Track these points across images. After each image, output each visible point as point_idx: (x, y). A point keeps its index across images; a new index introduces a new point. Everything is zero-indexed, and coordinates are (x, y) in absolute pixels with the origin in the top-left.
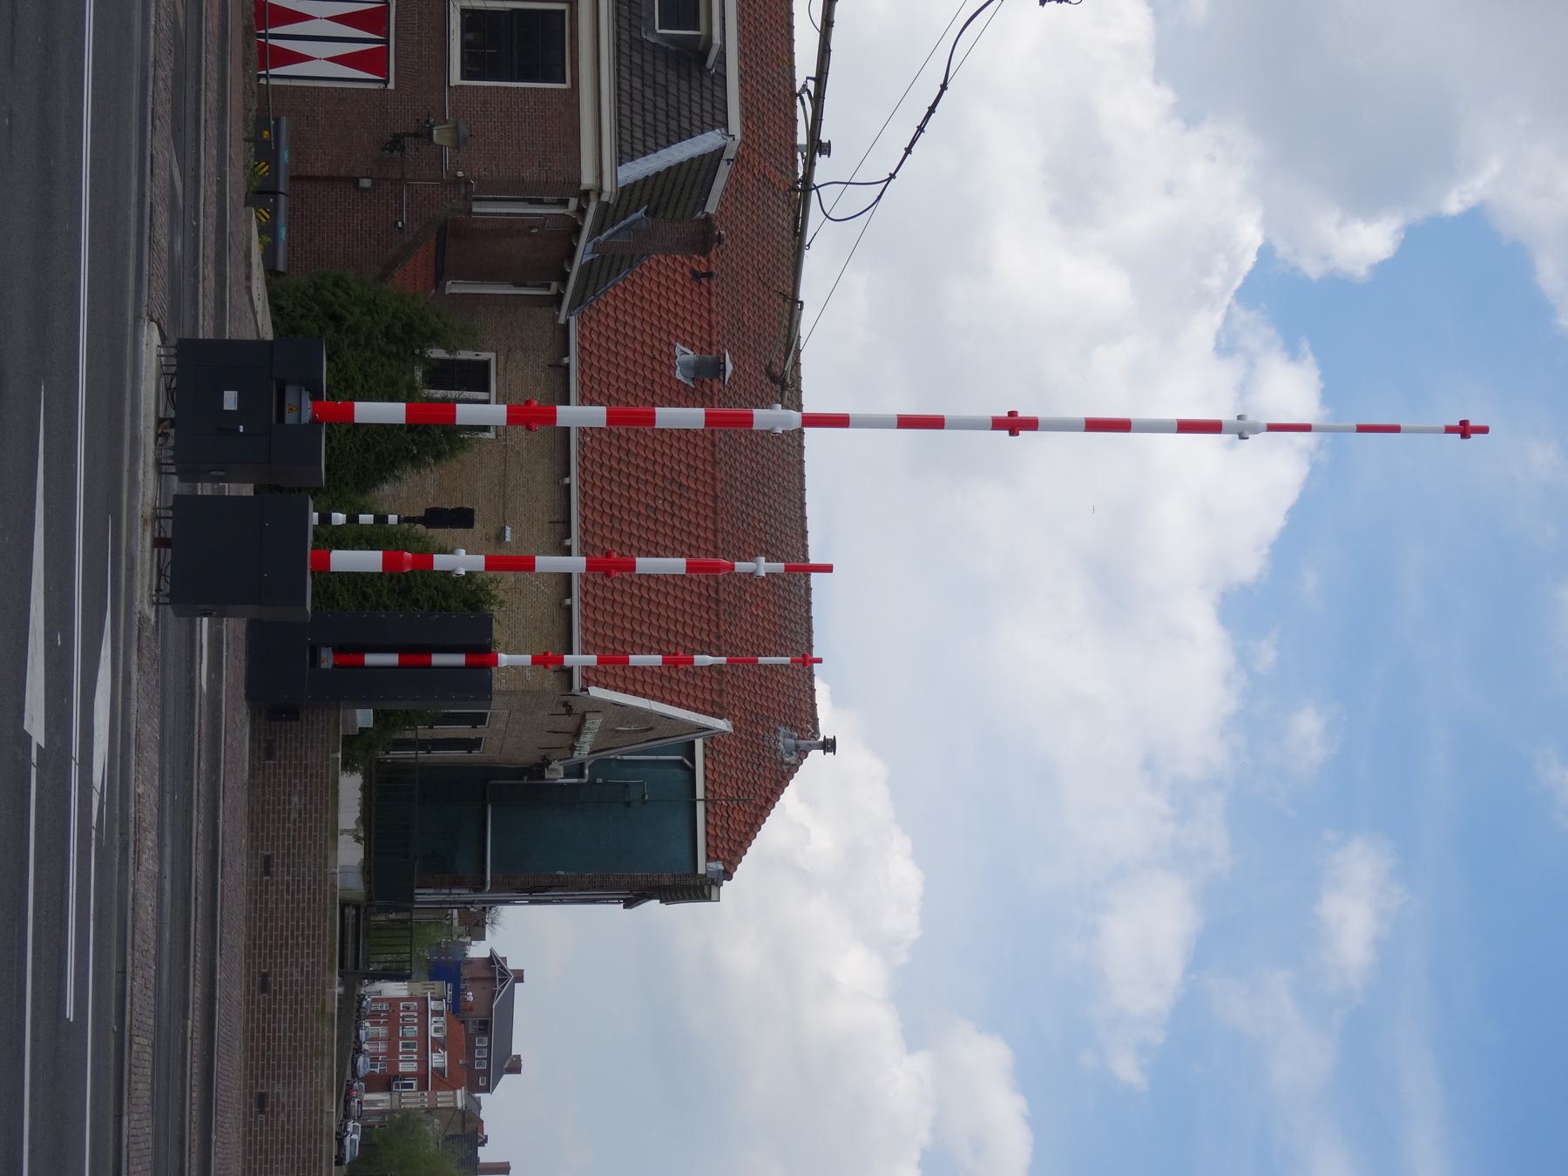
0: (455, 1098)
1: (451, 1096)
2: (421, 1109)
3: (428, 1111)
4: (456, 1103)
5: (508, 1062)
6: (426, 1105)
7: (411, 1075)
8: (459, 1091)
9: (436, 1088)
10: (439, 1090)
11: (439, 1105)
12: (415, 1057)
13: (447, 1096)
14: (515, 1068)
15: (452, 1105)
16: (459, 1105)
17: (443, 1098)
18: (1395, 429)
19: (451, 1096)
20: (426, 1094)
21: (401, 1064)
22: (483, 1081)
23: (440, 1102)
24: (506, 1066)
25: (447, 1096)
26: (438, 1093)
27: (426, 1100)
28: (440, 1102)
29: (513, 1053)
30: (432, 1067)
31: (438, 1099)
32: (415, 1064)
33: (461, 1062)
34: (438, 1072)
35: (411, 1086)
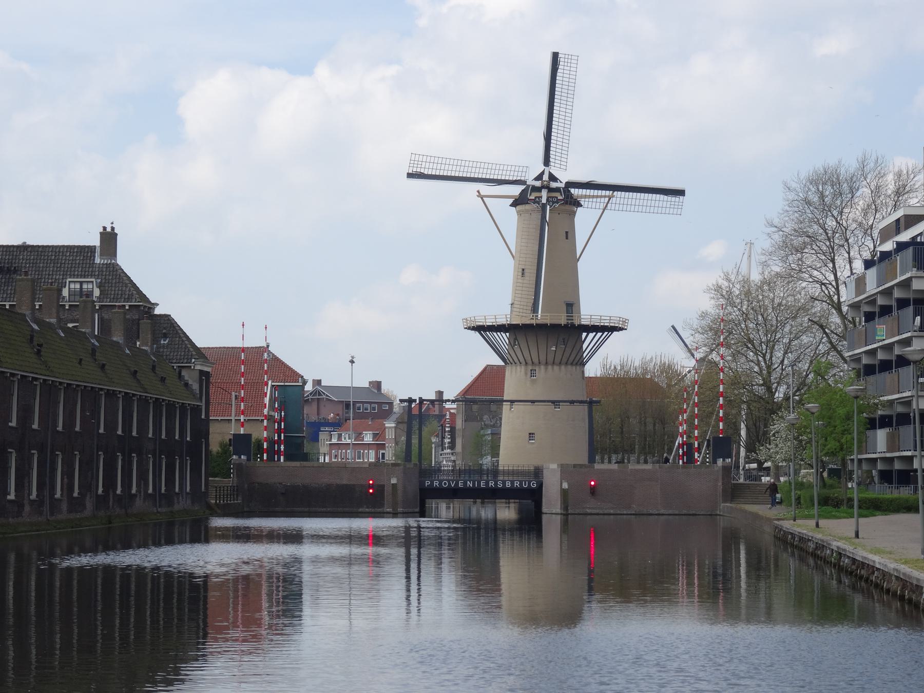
0: (390, 427)
1: (389, 430)
3: (397, 443)
4: (392, 427)
5: (373, 390)
7: (377, 454)
8: (386, 425)
10: (385, 436)
11: (393, 437)
12: (366, 451)
13: (389, 432)
14: (377, 385)
15: (393, 429)
16: (393, 425)
17: (390, 435)
19: (389, 430)
20: (387, 445)
21: (370, 460)
23: (392, 436)
24: (376, 391)
25: (389, 432)
26: (387, 438)
27: (390, 445)
28: (392, 436)
29: (368, 386)
30: (372, 441)
31: (390, 437)
32: (370, 451)
33: (370, 423)
34: (375, 436)
35: (383, 454)
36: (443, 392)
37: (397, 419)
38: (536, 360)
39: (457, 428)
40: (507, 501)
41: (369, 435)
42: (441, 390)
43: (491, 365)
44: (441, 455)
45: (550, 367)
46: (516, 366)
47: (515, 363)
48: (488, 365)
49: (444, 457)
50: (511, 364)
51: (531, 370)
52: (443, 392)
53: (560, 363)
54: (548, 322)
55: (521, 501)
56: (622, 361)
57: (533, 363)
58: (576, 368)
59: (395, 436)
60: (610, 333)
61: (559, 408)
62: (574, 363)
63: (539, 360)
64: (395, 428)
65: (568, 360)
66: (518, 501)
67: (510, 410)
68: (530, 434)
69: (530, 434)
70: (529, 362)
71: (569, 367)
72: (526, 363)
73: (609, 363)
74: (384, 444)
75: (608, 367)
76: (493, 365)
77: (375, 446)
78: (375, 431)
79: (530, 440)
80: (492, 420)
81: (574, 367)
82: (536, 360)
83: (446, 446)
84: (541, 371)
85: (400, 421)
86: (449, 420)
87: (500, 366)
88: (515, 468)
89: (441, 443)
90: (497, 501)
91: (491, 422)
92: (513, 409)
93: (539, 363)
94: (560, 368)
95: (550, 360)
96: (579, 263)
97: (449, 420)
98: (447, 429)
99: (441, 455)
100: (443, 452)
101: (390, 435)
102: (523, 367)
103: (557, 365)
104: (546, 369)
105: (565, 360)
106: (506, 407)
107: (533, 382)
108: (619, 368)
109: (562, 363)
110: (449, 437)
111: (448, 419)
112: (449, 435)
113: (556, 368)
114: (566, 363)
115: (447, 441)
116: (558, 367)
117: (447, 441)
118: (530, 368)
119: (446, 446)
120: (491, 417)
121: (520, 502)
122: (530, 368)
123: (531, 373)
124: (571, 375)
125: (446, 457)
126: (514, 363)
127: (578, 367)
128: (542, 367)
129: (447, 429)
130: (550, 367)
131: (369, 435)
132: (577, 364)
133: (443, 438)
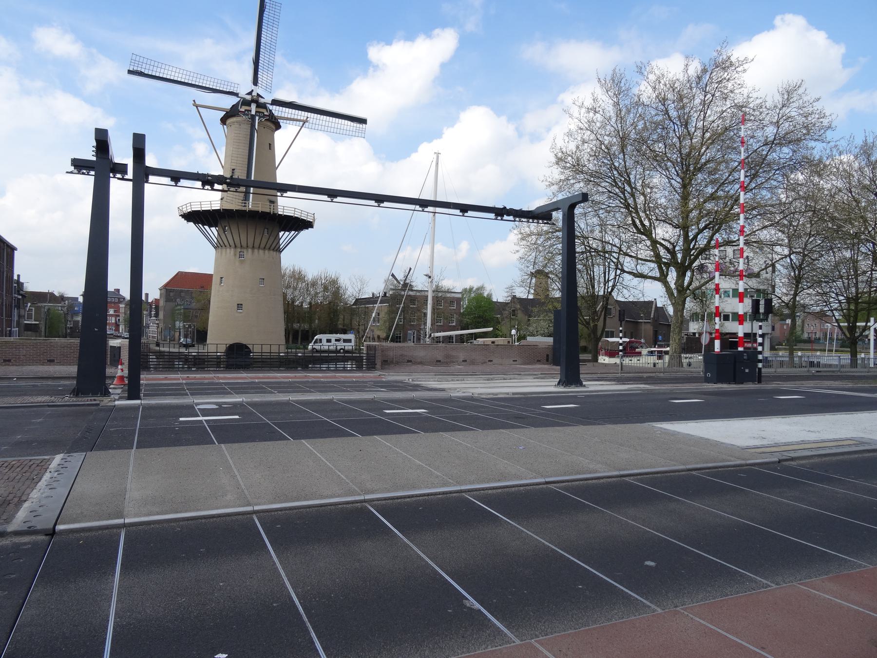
3: (125, 314)
16: (124, 306)
17: (122, 310)
34: (115, 311)
35: (119, 319)
38: (244, 244)
45: (256, 251)
46: (226, 249)
47: (225, 246)
53: (265, 248)
57: (241, 246)
62: (275, 249)
65: (271, 246)
69: (238, 304)
71: (272, 252)
79: (238, 309)
81: (275, 253)
82: (244, 244)
84: (248, 254)
92: (222, 284)
93: (247, 247)
94: (264, 253)
95: (257, 245)
96: (278, 171)
101: (122, 310)
102: (232, 249)
103: (262, 249)
104: (253, 252)
105: (268, 246)
107: (242, 262)
109: (266, 248)
113: (261, 251)
114: (269, 249)
115: (153, 313)
116: (263, 251)
118: (239, 250)
122: (239, 250)
123: (240, 255)
124: (273, 258)
126: (224, 246)
128: (250, 250)
130: (256, 251)
133: (151, 311)
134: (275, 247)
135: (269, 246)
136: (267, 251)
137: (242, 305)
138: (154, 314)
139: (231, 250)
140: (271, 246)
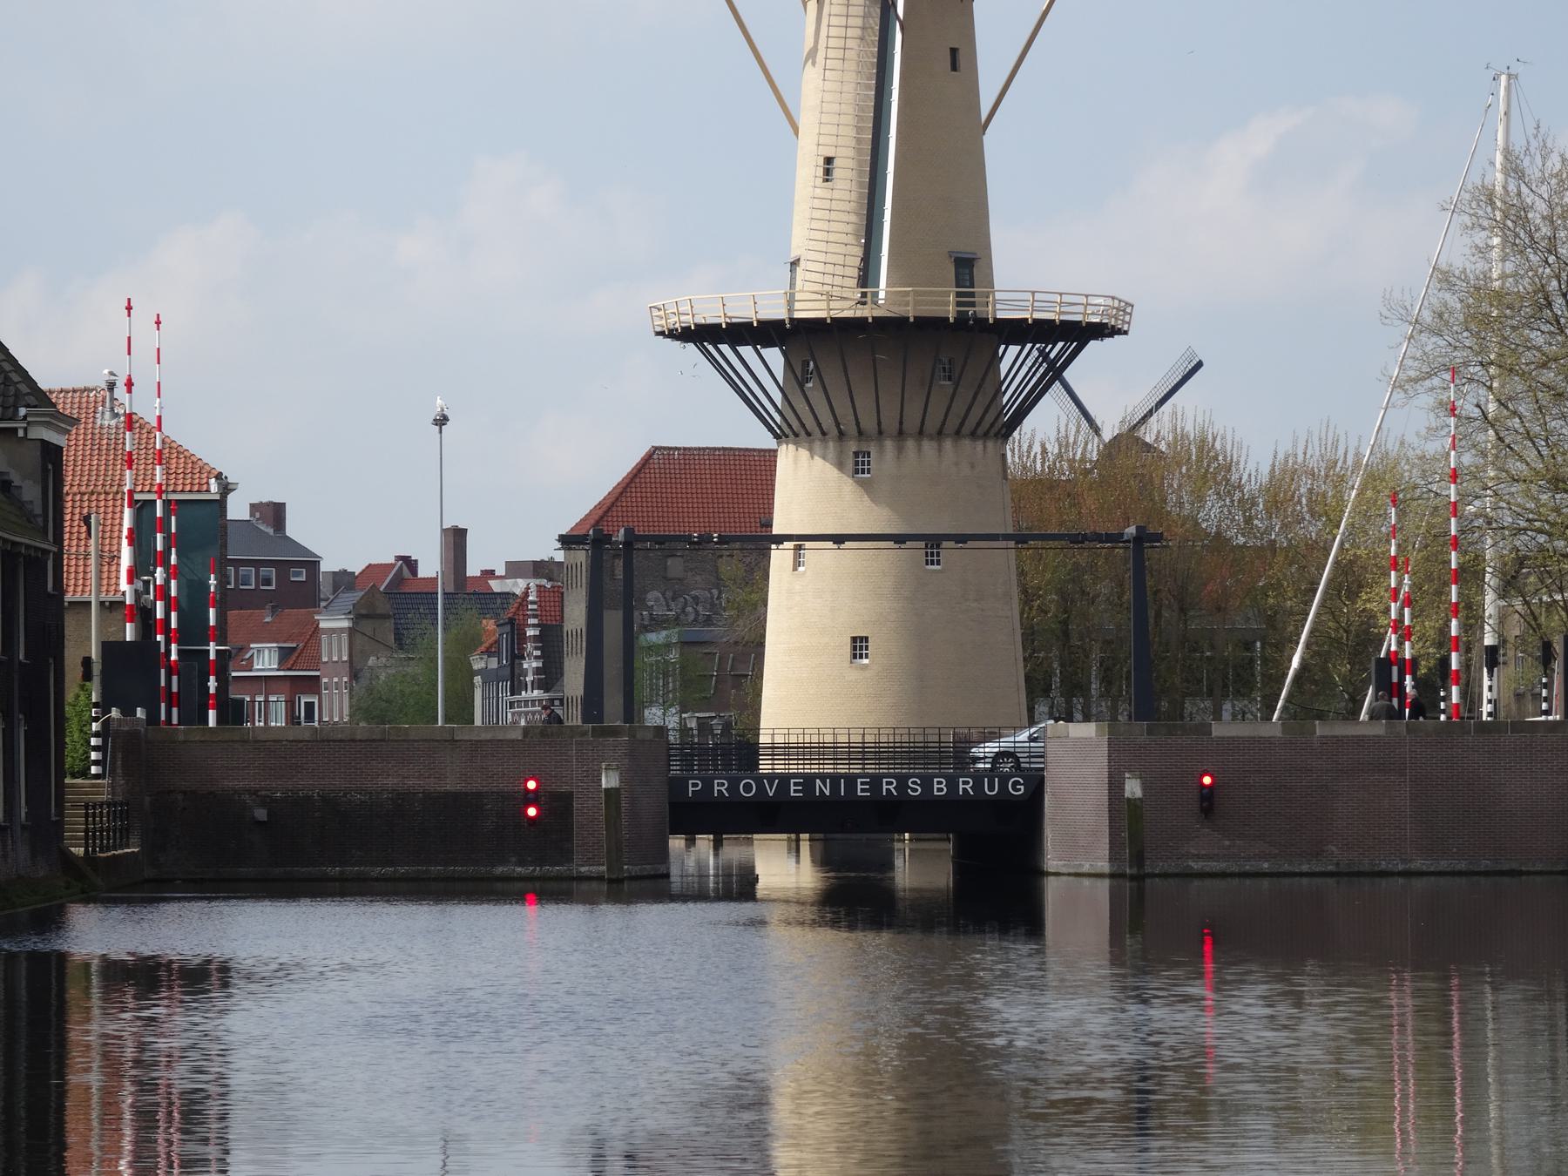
0: (333, 631)
1: (330, 638)
2: (352, 686)
3: (355, 675)
4: (342, 630)
5: (263, 527)
6: (345, 679)
7: (291, 705)
8: (322, 625)
9: (315, 662)
11: (345, 658)
12: (260, 698)
13: (330, 644)
15: (345, 636)
16: (346, 624)
17: (334, 651)
18: (129, 338)
19: (330, 638)
20: (325, 680)
22: (298, 574)
23: (340, 657)
24: (270, 531)
25: (330, 644)
26: (325, 659)
27: (336, 680)
28: (340, 657)
29: (247, 517)
30: (278, 670)
31: (335, 659)
32: (272, 698)
34: (285, 656)
35: (310, 706)
36: (464, 531)
37: (354, 605)
38: (869, 424)
39: (568, 626)
40: (793, 836)
41: (266, 652)
42: (460, 527)
43: (665, 448)
44: (512, 705)
45: (910, 444)
46: (813, 441)
47: (809, 434)
48: (656, 448)
49: (520, 714)
50: (796, 435)
51: (856, 454)
52: (464, 531)
53: (940, 433)
54: (910, 312)
55: (830, 836)
56: (1063, 430)
57: (860, 433)
58: (985, 447)
59: (350, 655)
60: (1050, 346)
61: (938, 564)
62: (980, 431)
63: (879, 423)
64: (351, 632)
65: (962, 424)
66: (821, 836)
67: (795, 569)
68: (854, 639)
69: (854, 639)
70: (851, 428)
71: (966, 443)
72: (841, 434)
73: (1029, 435)
74: (317, 677)
75: (1025, 447)
76: (670, 449)
77: (288, 684)
78: (285, 642)
79: (855, 656)
80: (673, 605)
81: (979, 445)
82: (869, 424)
83: (529, 678)
84: (884, 458)
85: (363, 612)
86: (535, 607)
87: (690, 449)
88: (793, 739)
89: (507, 671)
90: (755, 836)
91: (671, 610)
92: (801, 569)
93: (880, 432)
95: (912, 423)
96: (990, 140)
97: (535, 607)
98: (530, 632)
99: (512, 705)
100: (517, 697)
101: (334, 651)
102: (831, 444)
103: (931, 437)
104: (900, 450)
105: (953, 423)
106: (780, 558)
107: (866, 486)
108: (1053, 449)
109: (945, 431)
110: (538, 653)
111: (533, 603)
112: (536, 648)
113: (928, 446)
114: (958, 433)
115: (530, 665)
116: (934, 444)
117: (530, 665)
118: (852, 446)
119: (529, 678)
120: (669, 594)
121: (825, 840)
122: (852, 446)
123: (857, 463)
124: (973, 466)
125: (526, 713)
126: (803, 433)
127: (990, 444)
128: (889, 444)
129: (530, 632)
130: (910, 444)
131: (266, 652)
132: (986, 435)
133: (517, 656)
134: (979, 424)
135: (958, 422)
136: (948, 444)
137: (867, 638)
138: (537, 671)
139: (826, 448)
140: (962, 424)
